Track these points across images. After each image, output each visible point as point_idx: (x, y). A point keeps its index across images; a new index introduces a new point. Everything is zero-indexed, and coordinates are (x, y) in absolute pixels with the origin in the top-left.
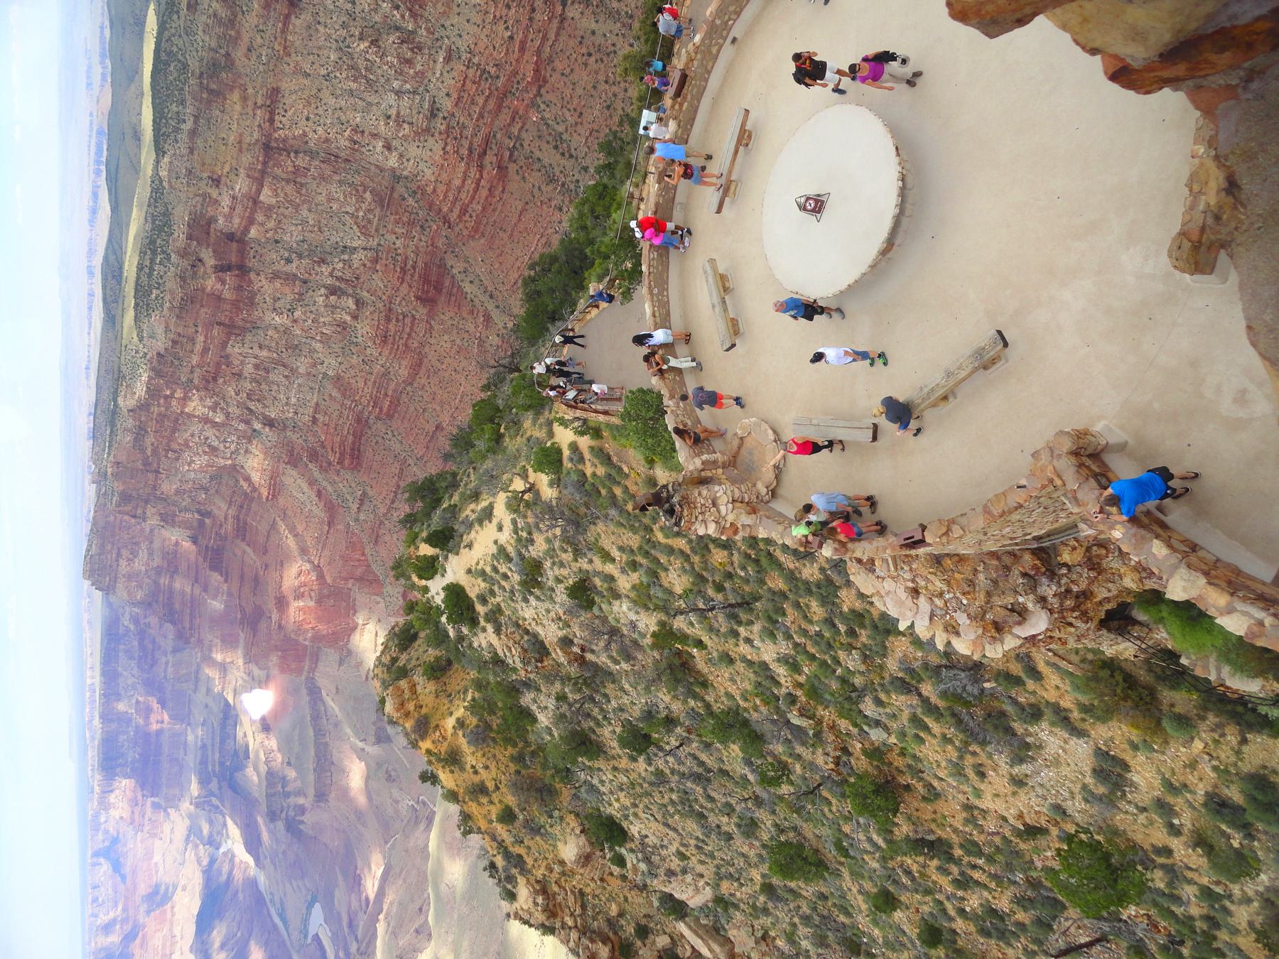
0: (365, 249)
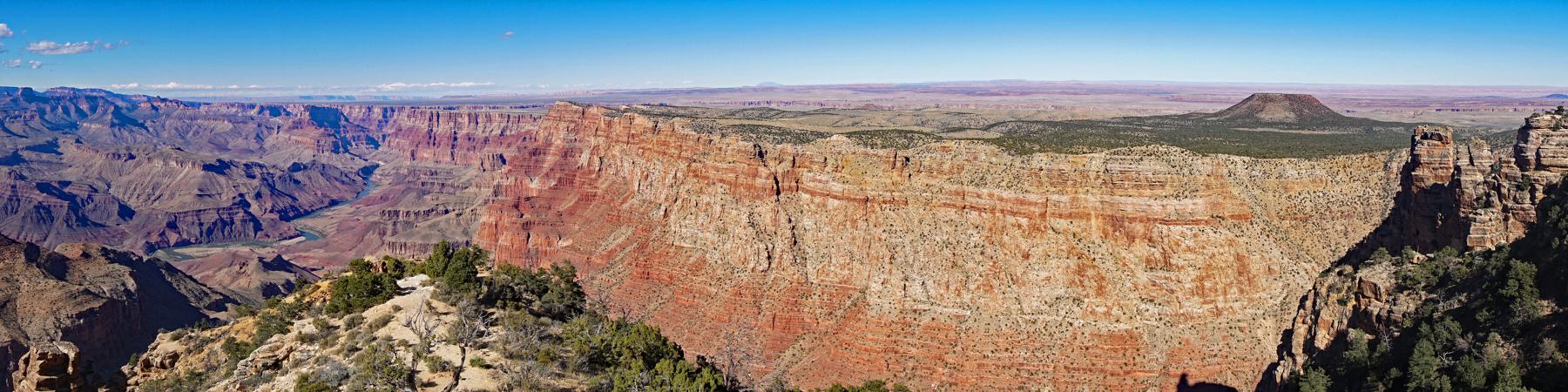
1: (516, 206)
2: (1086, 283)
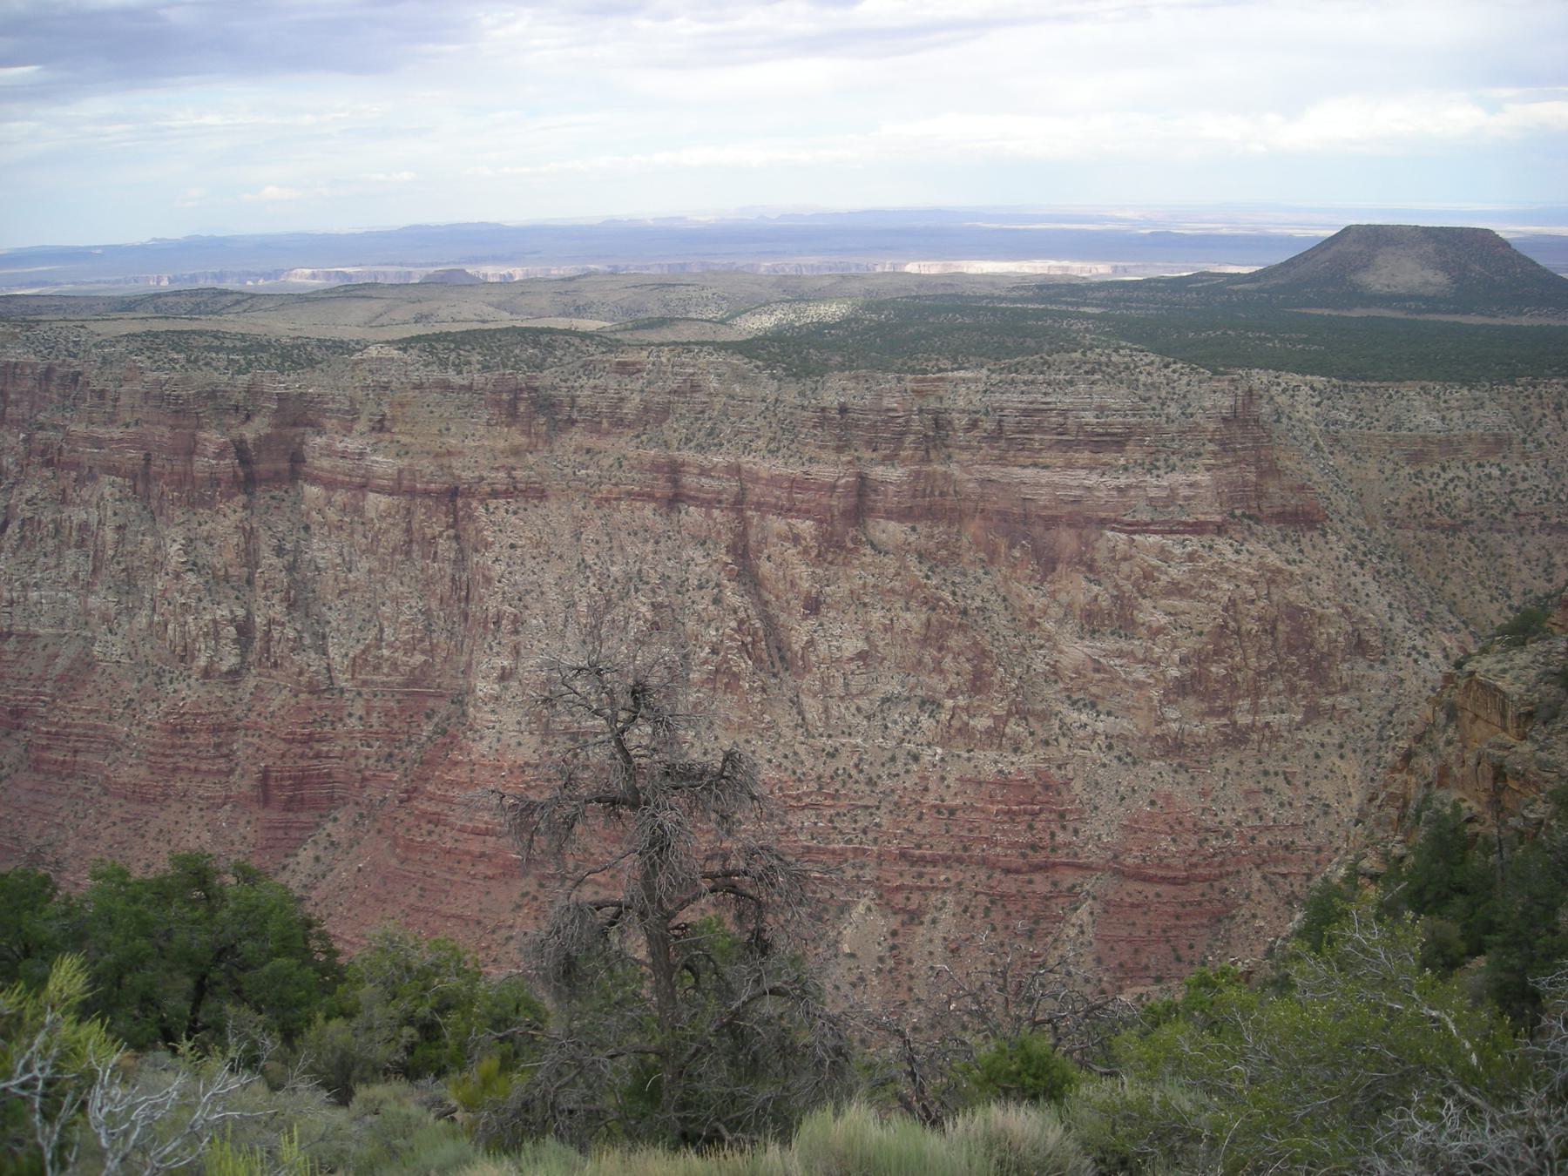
0: (329, 669)
2: (948, 662)
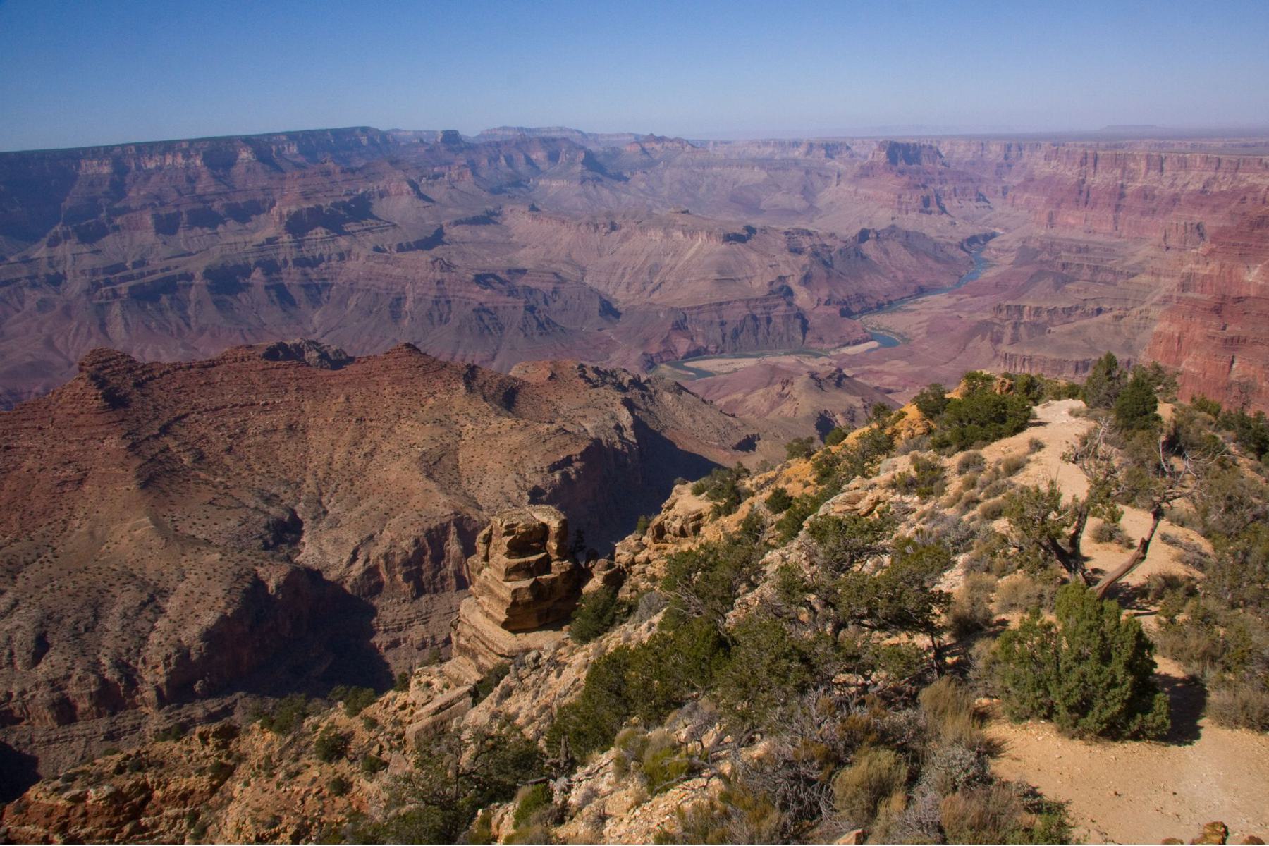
1: (1217, 310)
